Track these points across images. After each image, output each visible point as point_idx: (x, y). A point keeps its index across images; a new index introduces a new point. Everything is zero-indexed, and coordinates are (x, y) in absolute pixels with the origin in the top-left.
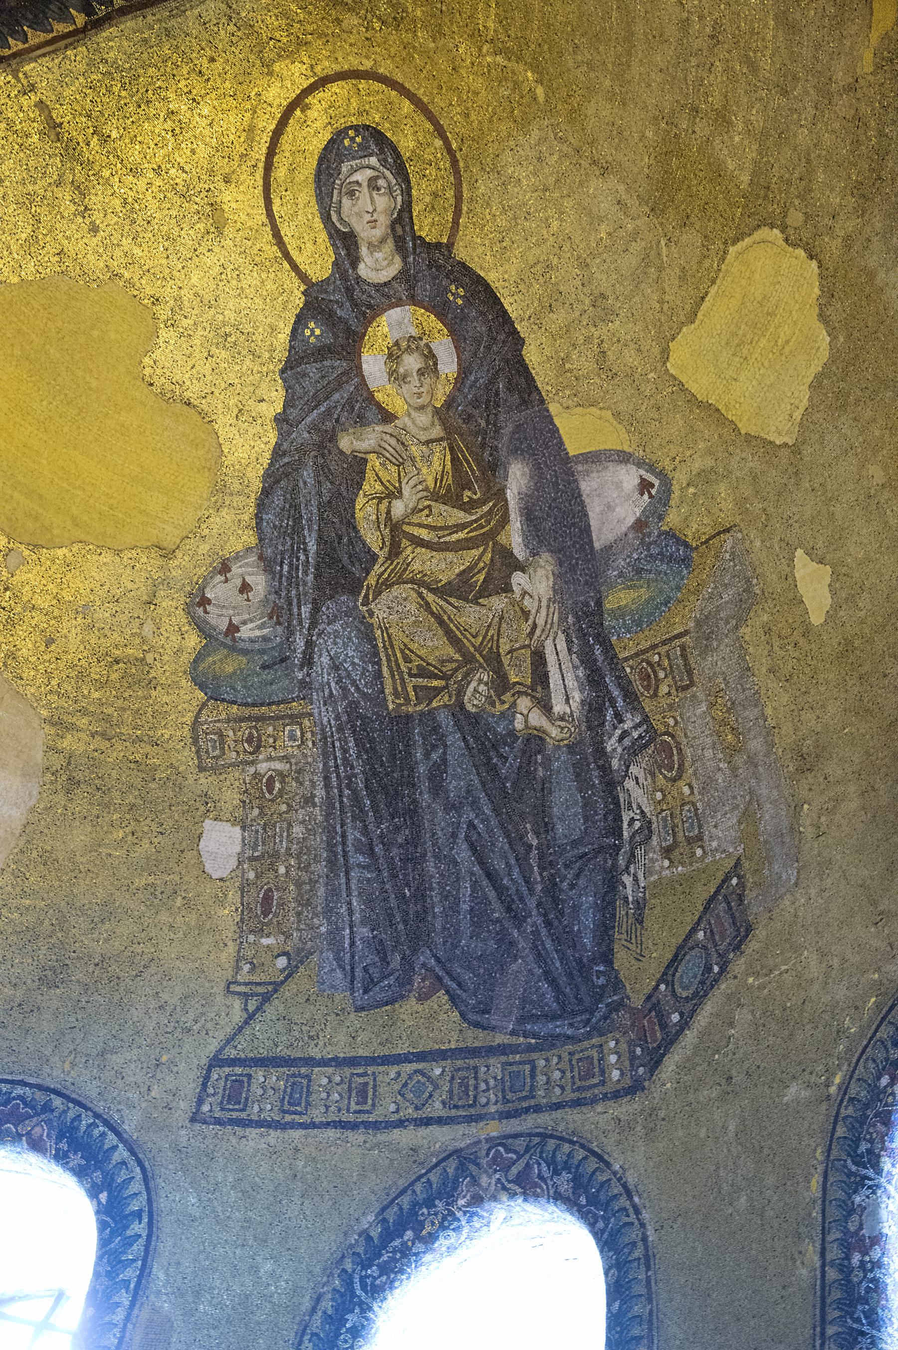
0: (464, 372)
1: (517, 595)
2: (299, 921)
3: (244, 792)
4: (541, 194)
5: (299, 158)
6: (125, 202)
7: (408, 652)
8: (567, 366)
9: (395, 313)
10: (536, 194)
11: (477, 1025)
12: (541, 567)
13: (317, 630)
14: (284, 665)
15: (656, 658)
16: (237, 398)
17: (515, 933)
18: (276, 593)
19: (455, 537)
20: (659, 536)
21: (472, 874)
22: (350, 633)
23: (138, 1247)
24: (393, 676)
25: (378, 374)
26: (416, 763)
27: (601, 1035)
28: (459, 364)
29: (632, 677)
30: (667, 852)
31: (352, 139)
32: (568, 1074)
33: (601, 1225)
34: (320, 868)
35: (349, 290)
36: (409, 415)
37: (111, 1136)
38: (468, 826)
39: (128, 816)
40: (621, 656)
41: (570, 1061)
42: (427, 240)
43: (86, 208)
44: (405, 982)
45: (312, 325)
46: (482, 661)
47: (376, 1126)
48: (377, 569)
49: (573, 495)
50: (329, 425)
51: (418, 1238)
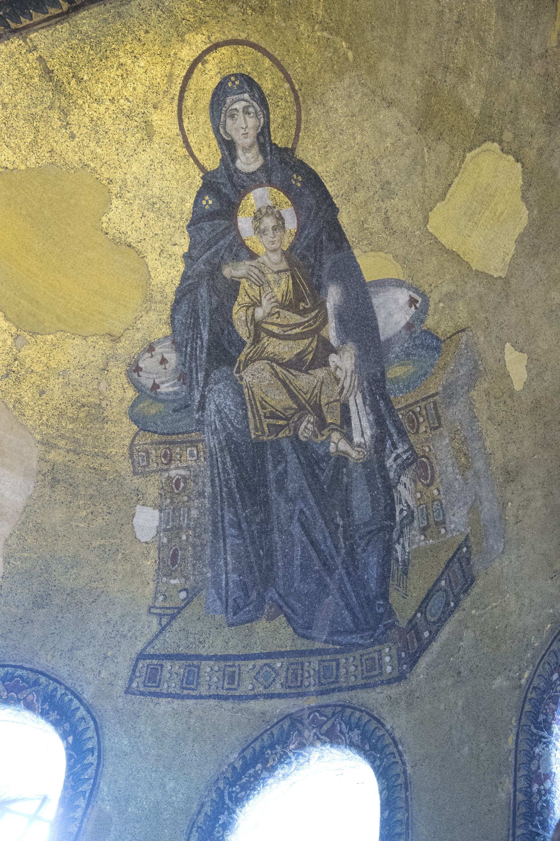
0: (301, 228)
2: (194, 570)
3: (162, 488)
4: (349, 118)
5: (200, 94)
6: (92, 120)
7: (264, 403)
8: (365, 226)
9: (259, 191)
10: (347, 118)
11: (303, 636)
12: (347, 351)
15: (418, 409)
16: (160, 242)
17: (328, 580)
18: (183, 364)
19: (294, 331)
20: (421, 333)
21: (302, 542)
22: (228, 390)
23: (91, 771)
24: (254, 417)
26: (268, 472)
27: (380, 644)
28: (298, 224)
29: (403, 421)
30: (423, 530)
31: (233, 83)
32: (360, 668)
33: (378, 763)
34: (208, 537)
35: (230, 177)
36: (267, 255)
37: (76, 702)
39: (89, 502)
40: (396, 407)
41: (361, 660)
42: (279, 146)
43: (68, 124)
44: (259, 608)
45: (207, 198)
46: (309, 408)
47: (239, 698)
48: (246, 350)
50: (217, 260)
51: (265, 768)
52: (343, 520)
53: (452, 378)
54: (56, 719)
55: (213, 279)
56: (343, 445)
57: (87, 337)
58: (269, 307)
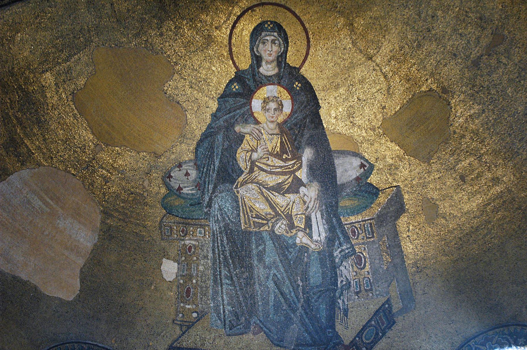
1: (302, 194)
2: (201, 301)
7: (251, 208)
9: (271, 87)
14: (199, 205)
15: (359, 226)
17: (292, 315)
18: (200, 178)
21: (275, 292)
24: (245, 216)
25: (258, 107)
26: (252, 249)
28: (292, 110)
30: (357, 293)
34: (210, 283)
35: (254, 75)
36: (266, 123)
38: (273, 275)
44: (247, 327)
45: (235, 84)
46: (284, 216)
49: (331, 164)
52: (302, 282)
53: (385, 212)
55: (227, 131)
56: (306, 240)
57: (140, 152)
58: (262, 153)
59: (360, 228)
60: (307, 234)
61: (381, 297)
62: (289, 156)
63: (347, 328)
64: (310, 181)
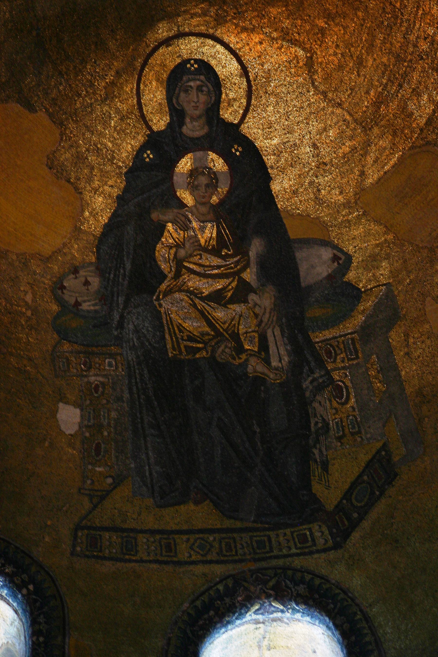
4: (298, 109)
9: (199, 154)
11: (230, 517)
13: (127, 310)
15: (336, 343)
18: (105, 288)
24: (172, 339)
27: (310, 523)
28: (231, 185)
30: (339, 439)
46: (227, 336)
47: (180, 563)
54: (13, 571)
59: (337, 346)
60: (263, 359)
61: (374, 441)
62: (230, 251)
63: (328, 487)
64: (263, 285)
